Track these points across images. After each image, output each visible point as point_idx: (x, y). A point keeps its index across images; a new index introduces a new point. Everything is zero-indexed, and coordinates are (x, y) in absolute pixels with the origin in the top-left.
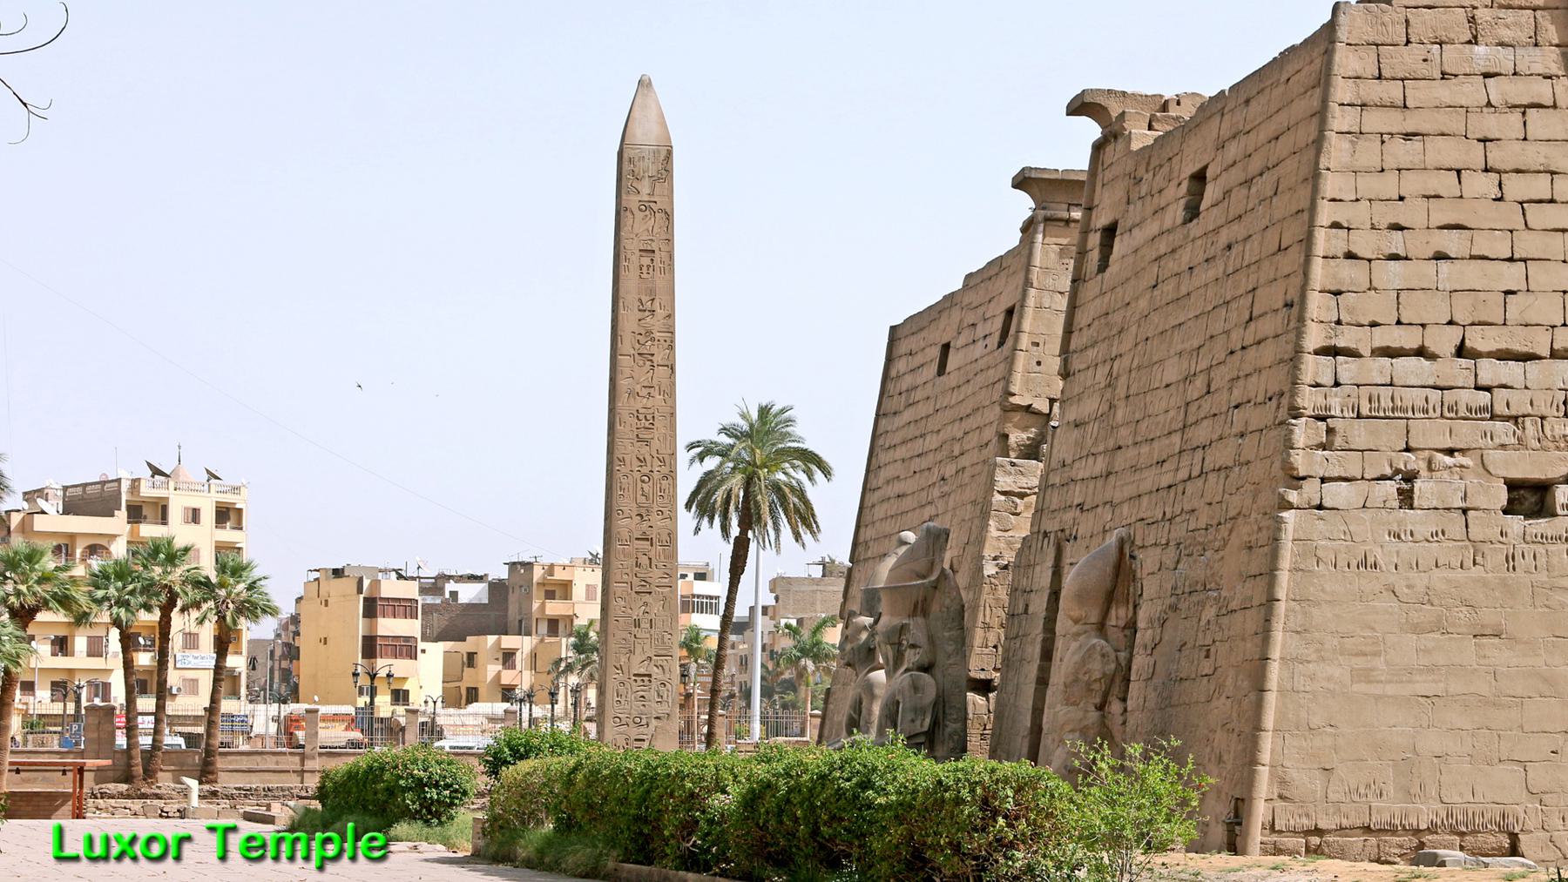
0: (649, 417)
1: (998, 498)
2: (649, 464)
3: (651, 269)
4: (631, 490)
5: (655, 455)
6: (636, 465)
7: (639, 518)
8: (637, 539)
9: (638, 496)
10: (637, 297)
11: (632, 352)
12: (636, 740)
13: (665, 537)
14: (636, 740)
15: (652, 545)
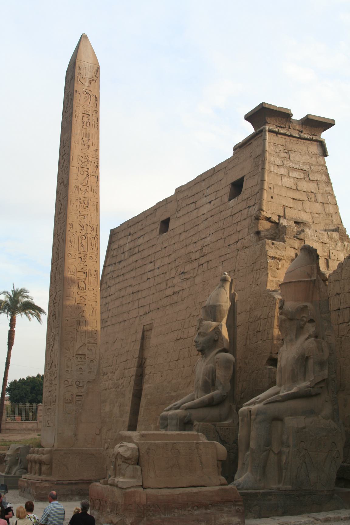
0: (86, 203)
1: (269, 260)
2: (85, 229)
3: (88, 124)
4: (76, 241)
5: (88, 223)
6: (79, 228)
7: (80, 259)
9: (80, 247)
10: (81, 137)
11: (77, 166)
12: (77, 395)
13: (93, 273)
14: (77, 395)
15: (86, 276)
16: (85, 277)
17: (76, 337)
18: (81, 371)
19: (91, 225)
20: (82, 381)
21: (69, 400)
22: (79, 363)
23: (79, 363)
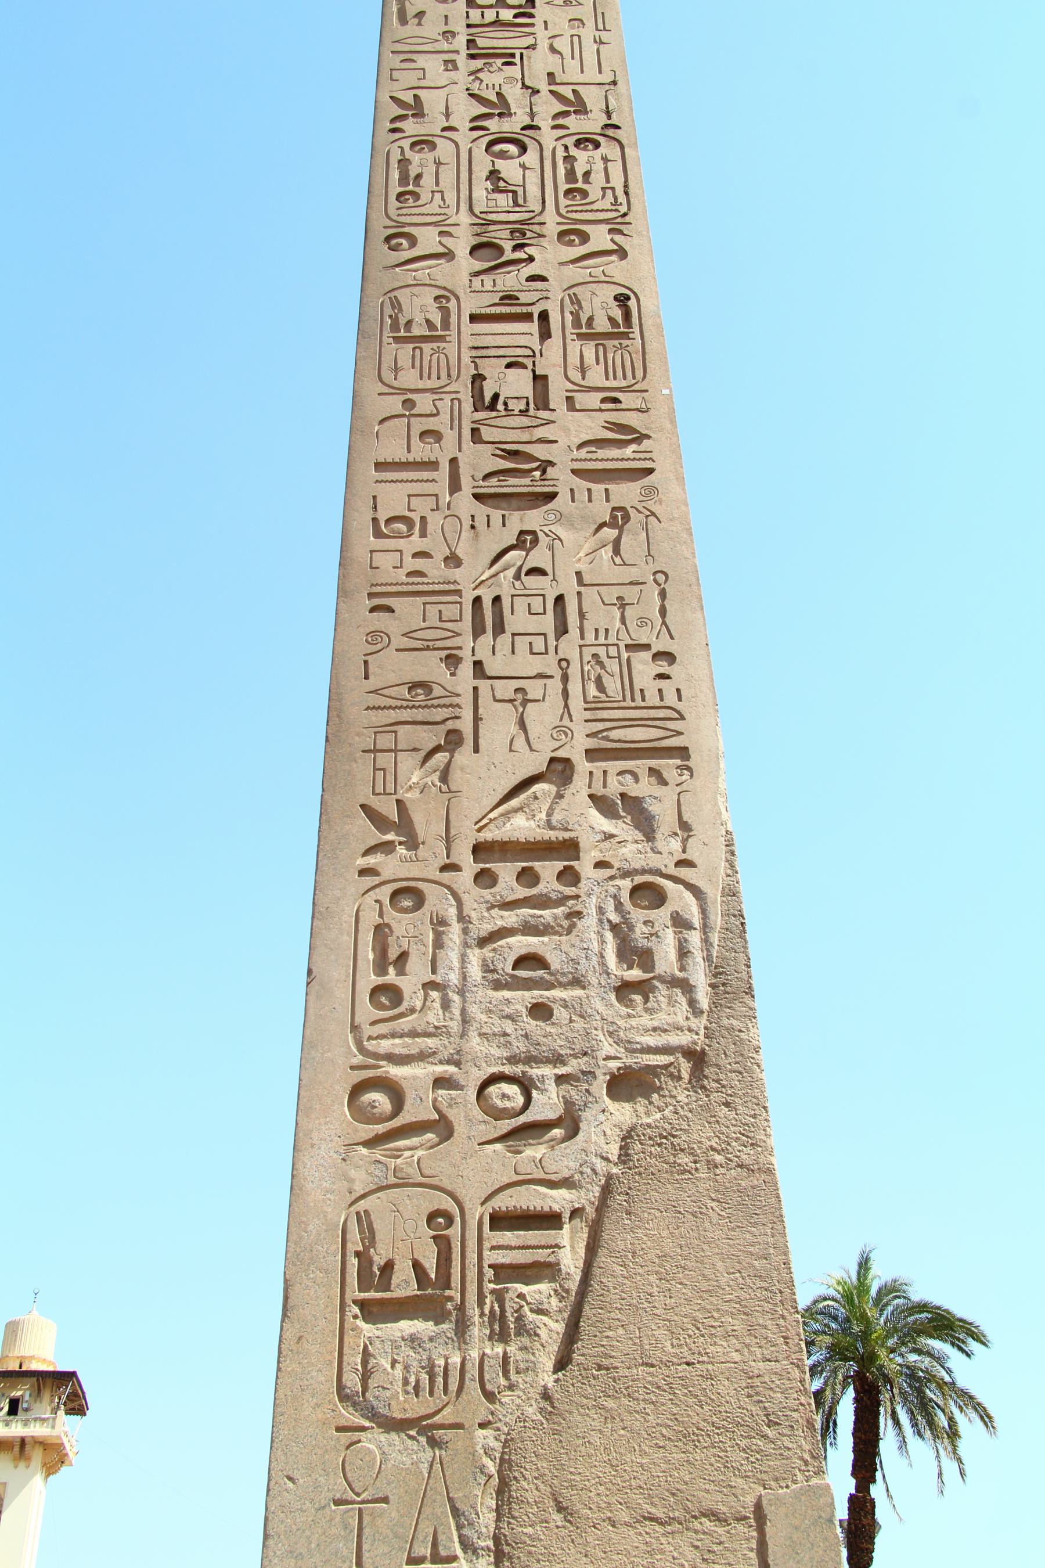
8: (474, 318)
12: (500, 1221)
14: (500, 1221)
16: (534, 342)
17: (467, 714)
18: (528, 985)
19: (567, 92)
20: (548, 1071)
21: (405, 1272)
22: (510, 918)
23: (510, 918)
